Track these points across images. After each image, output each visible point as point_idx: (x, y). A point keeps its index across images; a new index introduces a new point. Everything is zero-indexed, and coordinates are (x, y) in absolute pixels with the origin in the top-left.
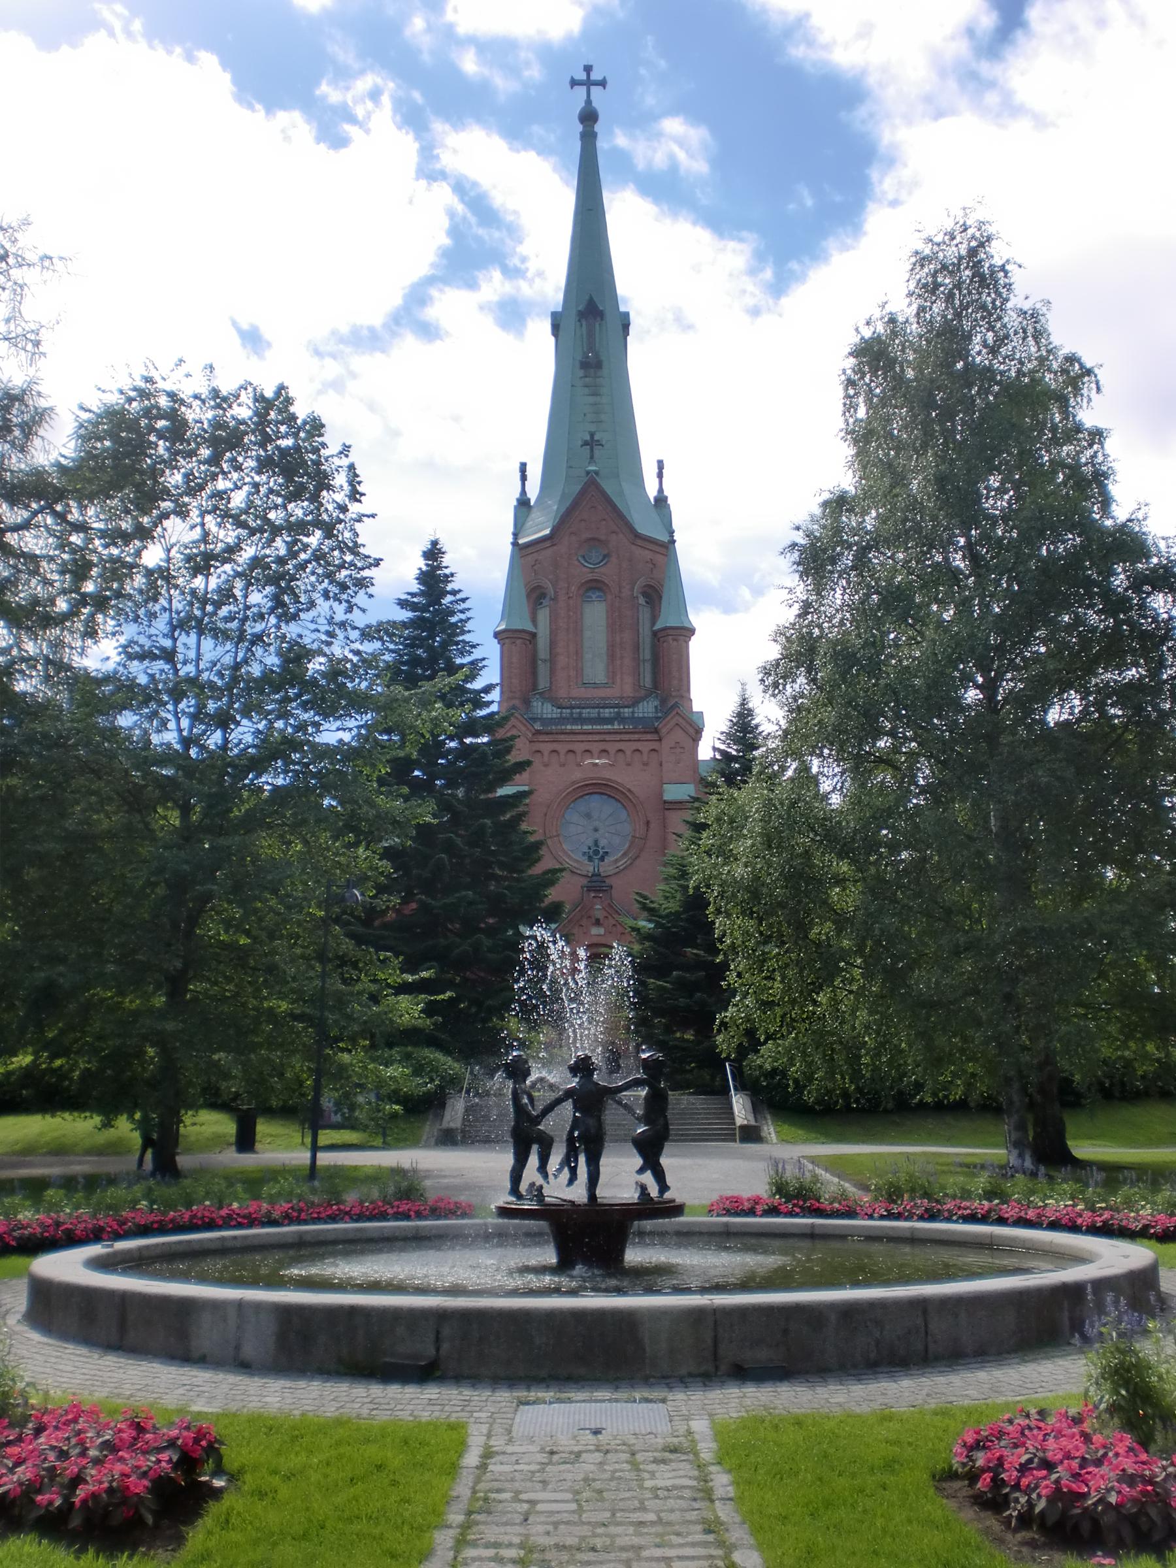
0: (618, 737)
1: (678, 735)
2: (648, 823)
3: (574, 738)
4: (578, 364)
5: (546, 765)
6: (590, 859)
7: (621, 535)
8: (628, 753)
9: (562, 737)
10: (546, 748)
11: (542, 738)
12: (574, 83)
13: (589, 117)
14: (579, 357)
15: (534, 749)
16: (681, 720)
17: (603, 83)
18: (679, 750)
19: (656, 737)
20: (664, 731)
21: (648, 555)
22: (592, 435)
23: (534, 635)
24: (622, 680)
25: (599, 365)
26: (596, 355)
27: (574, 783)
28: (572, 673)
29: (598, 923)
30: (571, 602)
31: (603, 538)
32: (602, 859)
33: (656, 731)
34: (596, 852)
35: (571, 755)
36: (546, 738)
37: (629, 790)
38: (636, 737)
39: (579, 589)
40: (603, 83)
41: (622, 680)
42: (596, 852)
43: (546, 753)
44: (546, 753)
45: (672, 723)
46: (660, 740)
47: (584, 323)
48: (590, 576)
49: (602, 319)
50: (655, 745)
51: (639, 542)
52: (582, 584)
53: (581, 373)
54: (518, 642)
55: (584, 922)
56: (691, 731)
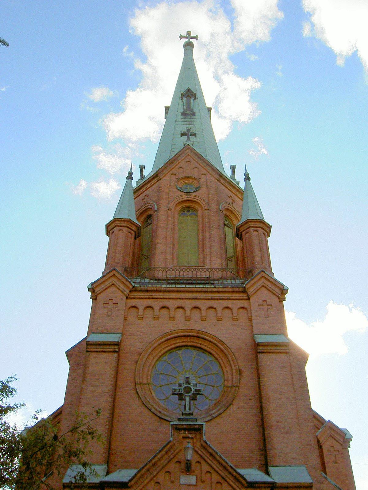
0: (210, 295)
1: (264, 295)
2: (240, 372)
3: (167, 295)
4: (180, 114)
5: (141, 318)
6: (181, 397)
7: (209, 176)
8: (219, 309)
9: (157, 295)
10: (141, 304)
11: (137, 294)
12: (181, 37)
13: (189, 46)
14: (181, 110)
15: (131, 305)
16: (266, 282)
17: (196, 38)
18: (266, 307)
19: (244, 296)
20: (251, 291)
21: (230, 194)
22: (188, 130)
23: (139, 228)
24: (211, 261)
25: (194, 114)
26: (192, 110)
27: (166, 334)
28: (168, 256)
29: (188, 468)
30: (170, 212)
31: (197, 177)
32: (194, 398)
33: (245, 291)
34: (188, 390)
35: (164, 311)
36: (142, 295)
37: (221, 342)
38: (226, 295)
39: (176, 206)
40: (196, 38)
41: (211, 261)
42: (188, 390)
43: (141, 309)
44: (141, 309)
45: (260, 283)
46: (249, 299)
47: (184, 99)
48: (185, 197)
49: (195, 98)
50: (244, 303)
51: (221, 180)
52: (180, 203)
53: (183, 117)
54: (125, 229)
55: (172, 467)
56: (278, 291)
